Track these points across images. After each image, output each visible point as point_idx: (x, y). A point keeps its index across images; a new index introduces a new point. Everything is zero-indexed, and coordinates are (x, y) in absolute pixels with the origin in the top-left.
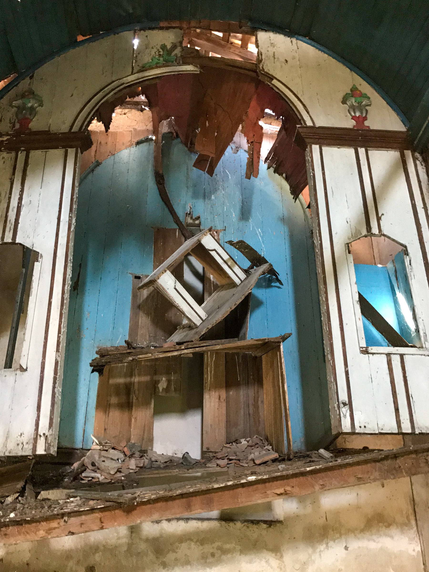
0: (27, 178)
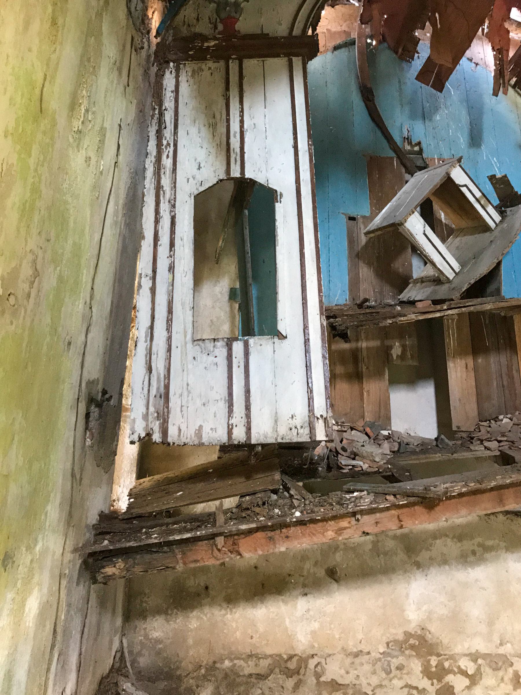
0: (244, 95)
